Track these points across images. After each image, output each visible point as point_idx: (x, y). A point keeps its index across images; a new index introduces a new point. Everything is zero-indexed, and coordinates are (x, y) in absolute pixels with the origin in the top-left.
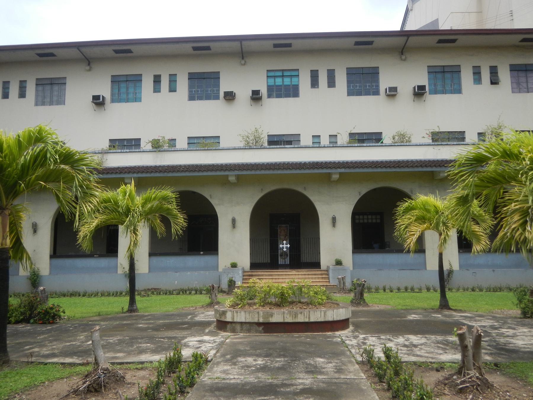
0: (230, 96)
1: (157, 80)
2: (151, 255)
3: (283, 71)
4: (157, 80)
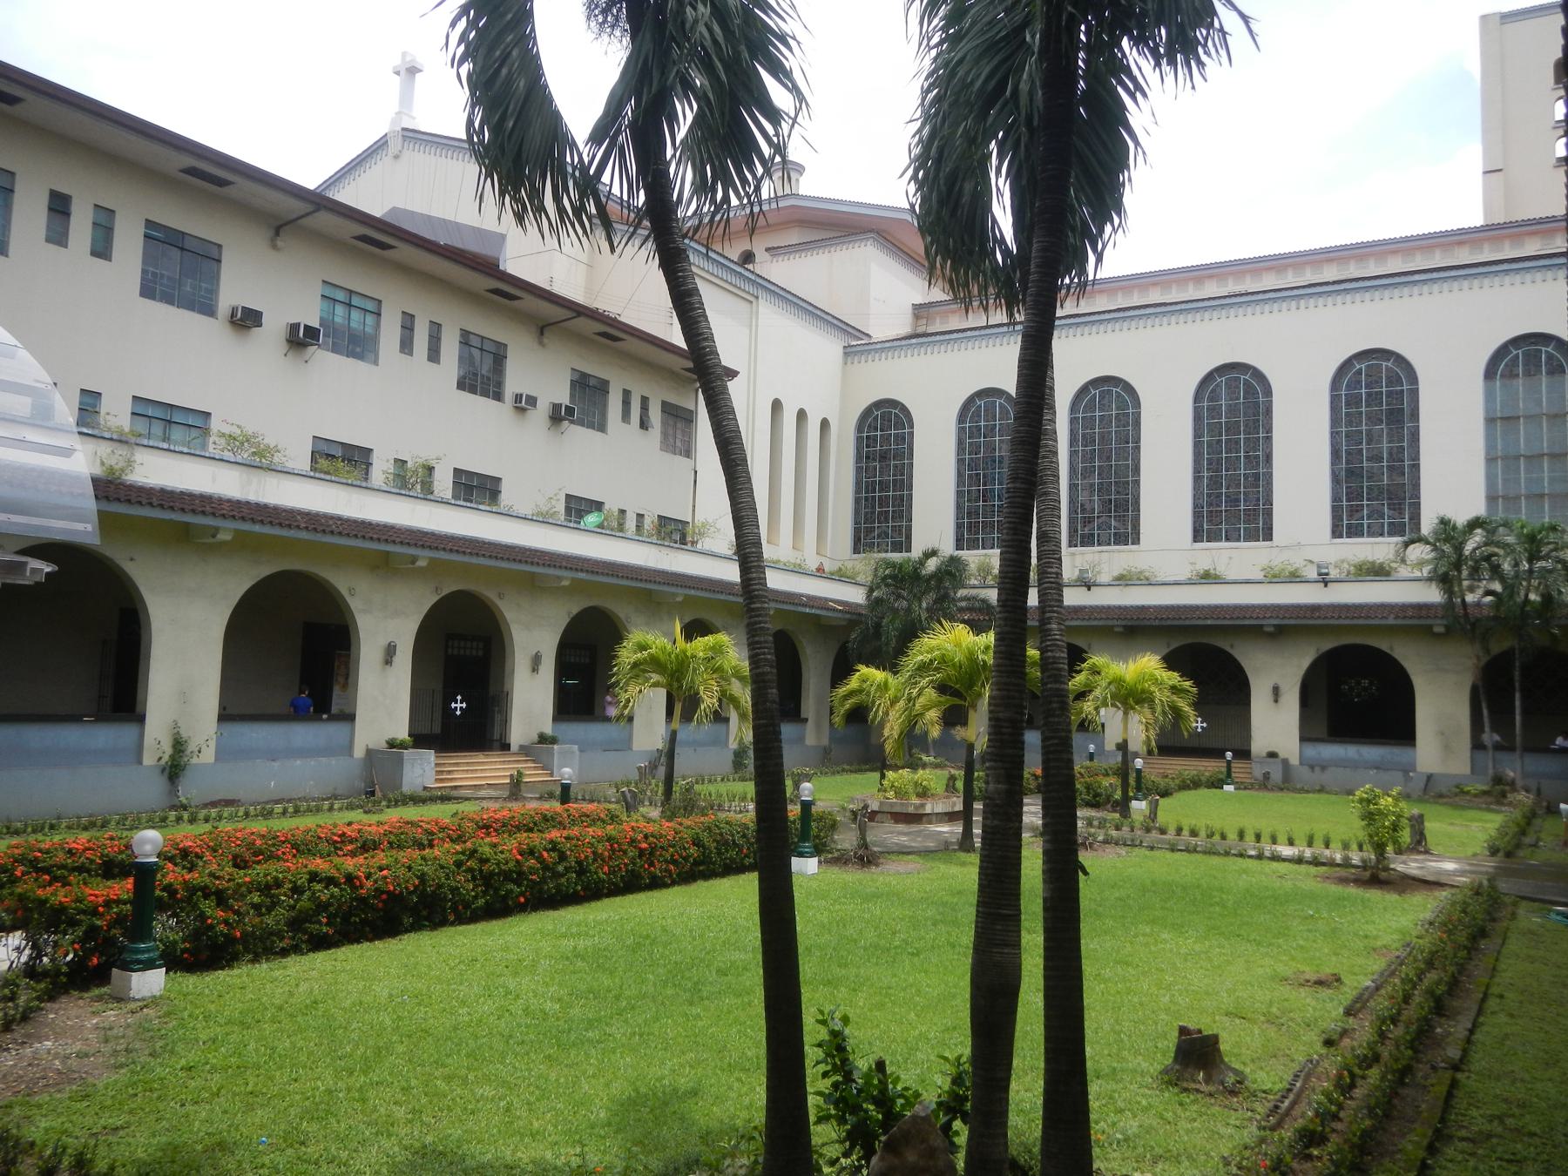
0: (246, 320)
1: (59, 206)
2: (225, 716)
3: (351, 292)
4: (59, 206)
